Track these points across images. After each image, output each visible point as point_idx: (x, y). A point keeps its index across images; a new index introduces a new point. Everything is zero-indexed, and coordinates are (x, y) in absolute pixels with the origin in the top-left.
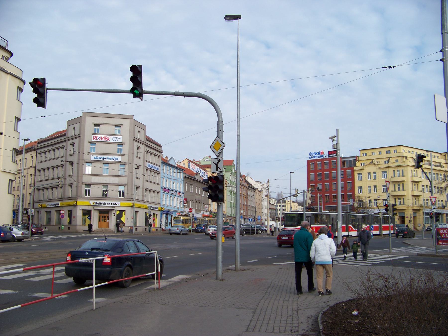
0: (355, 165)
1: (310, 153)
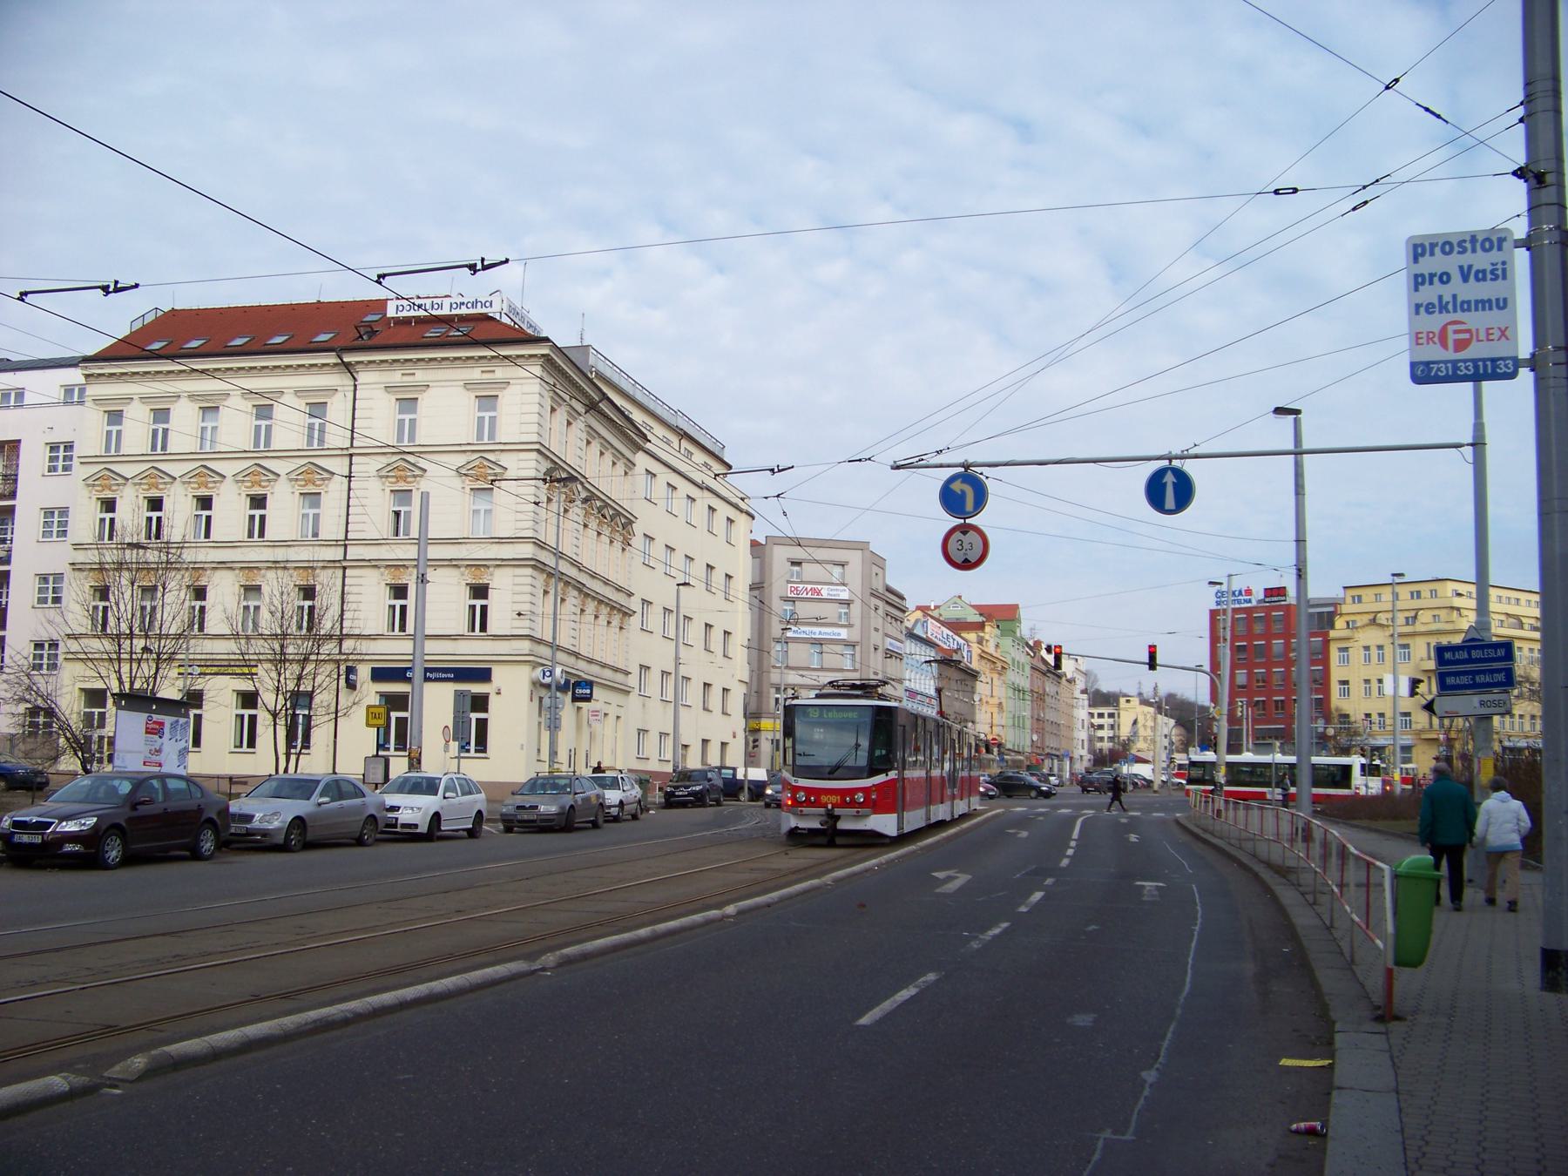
0: (1332, 626)
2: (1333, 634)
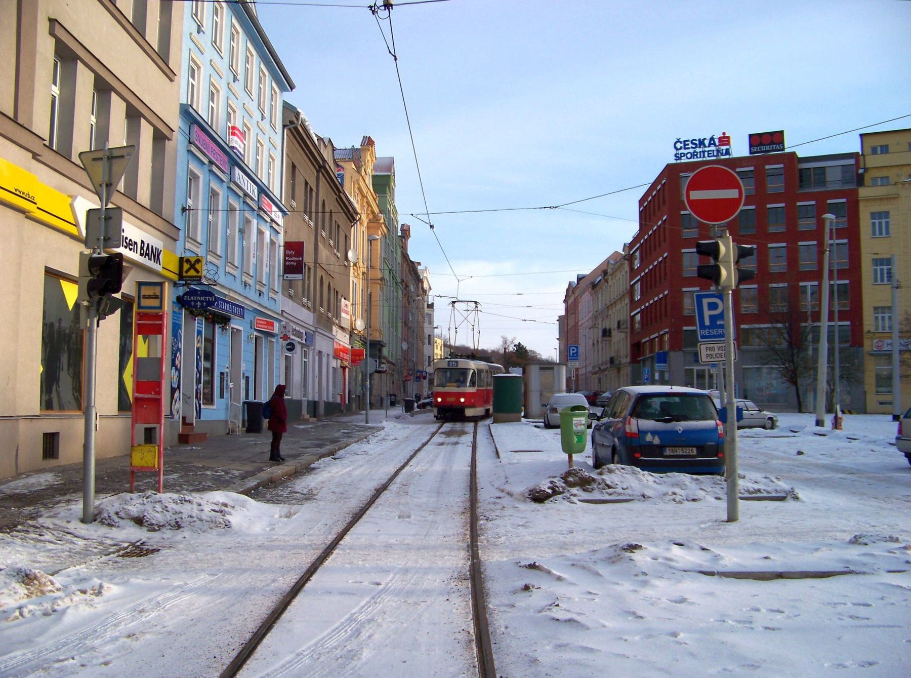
1: (678, 141)
2: (863, 192)
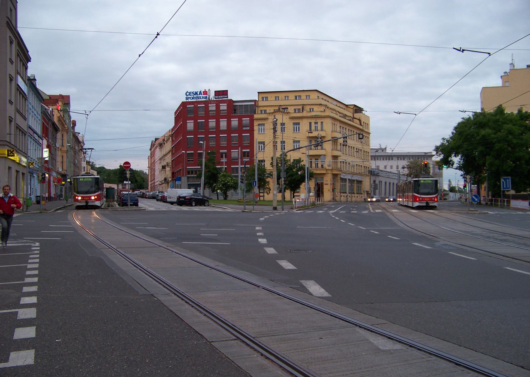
1: (187, 92)
2: (256, 116)
